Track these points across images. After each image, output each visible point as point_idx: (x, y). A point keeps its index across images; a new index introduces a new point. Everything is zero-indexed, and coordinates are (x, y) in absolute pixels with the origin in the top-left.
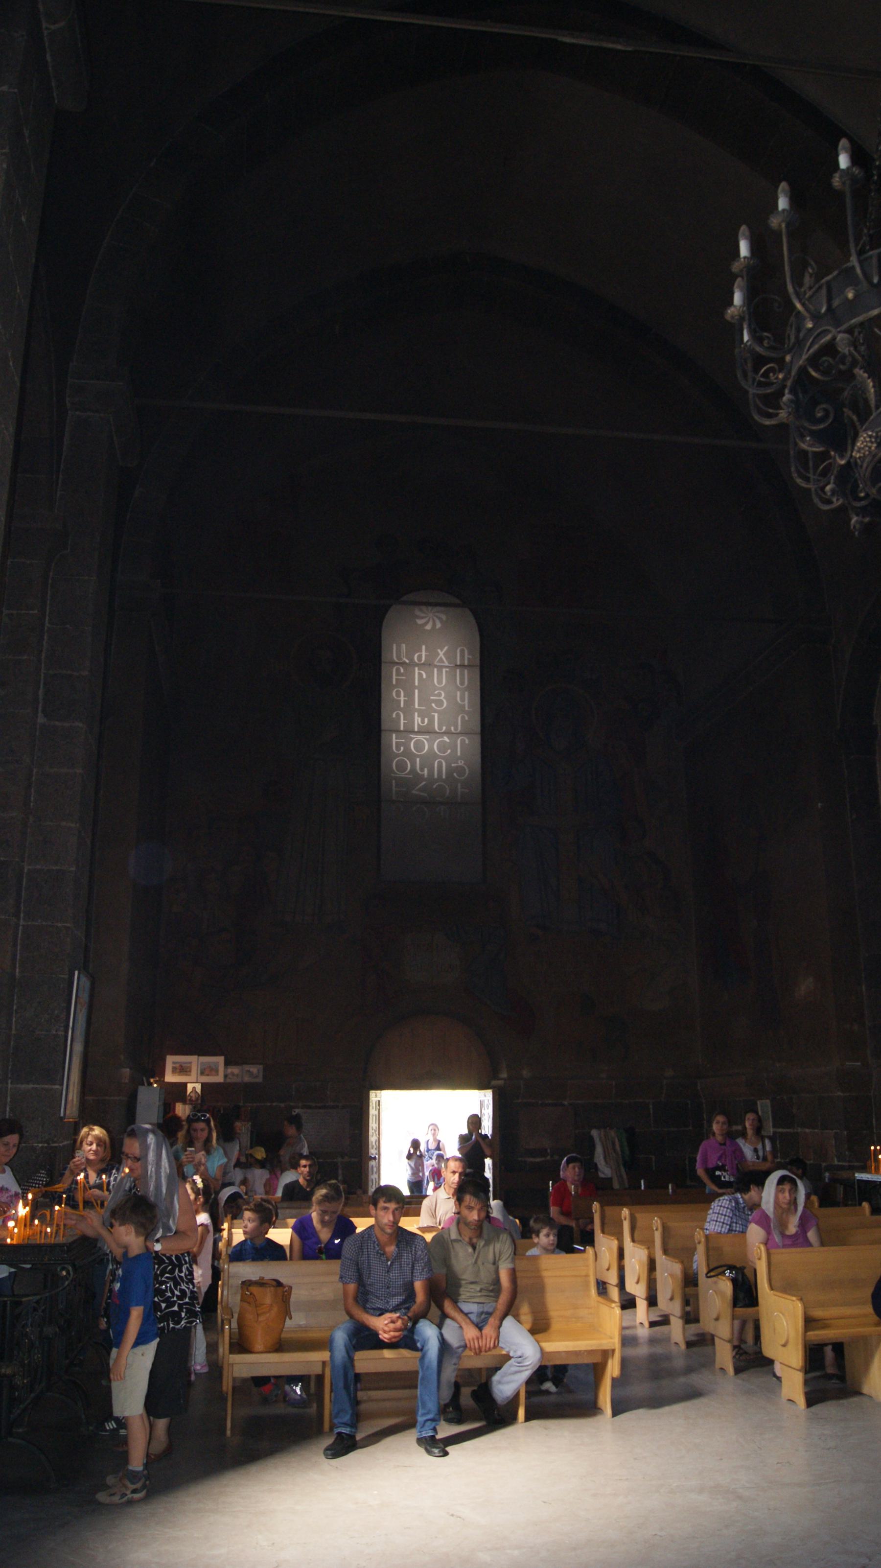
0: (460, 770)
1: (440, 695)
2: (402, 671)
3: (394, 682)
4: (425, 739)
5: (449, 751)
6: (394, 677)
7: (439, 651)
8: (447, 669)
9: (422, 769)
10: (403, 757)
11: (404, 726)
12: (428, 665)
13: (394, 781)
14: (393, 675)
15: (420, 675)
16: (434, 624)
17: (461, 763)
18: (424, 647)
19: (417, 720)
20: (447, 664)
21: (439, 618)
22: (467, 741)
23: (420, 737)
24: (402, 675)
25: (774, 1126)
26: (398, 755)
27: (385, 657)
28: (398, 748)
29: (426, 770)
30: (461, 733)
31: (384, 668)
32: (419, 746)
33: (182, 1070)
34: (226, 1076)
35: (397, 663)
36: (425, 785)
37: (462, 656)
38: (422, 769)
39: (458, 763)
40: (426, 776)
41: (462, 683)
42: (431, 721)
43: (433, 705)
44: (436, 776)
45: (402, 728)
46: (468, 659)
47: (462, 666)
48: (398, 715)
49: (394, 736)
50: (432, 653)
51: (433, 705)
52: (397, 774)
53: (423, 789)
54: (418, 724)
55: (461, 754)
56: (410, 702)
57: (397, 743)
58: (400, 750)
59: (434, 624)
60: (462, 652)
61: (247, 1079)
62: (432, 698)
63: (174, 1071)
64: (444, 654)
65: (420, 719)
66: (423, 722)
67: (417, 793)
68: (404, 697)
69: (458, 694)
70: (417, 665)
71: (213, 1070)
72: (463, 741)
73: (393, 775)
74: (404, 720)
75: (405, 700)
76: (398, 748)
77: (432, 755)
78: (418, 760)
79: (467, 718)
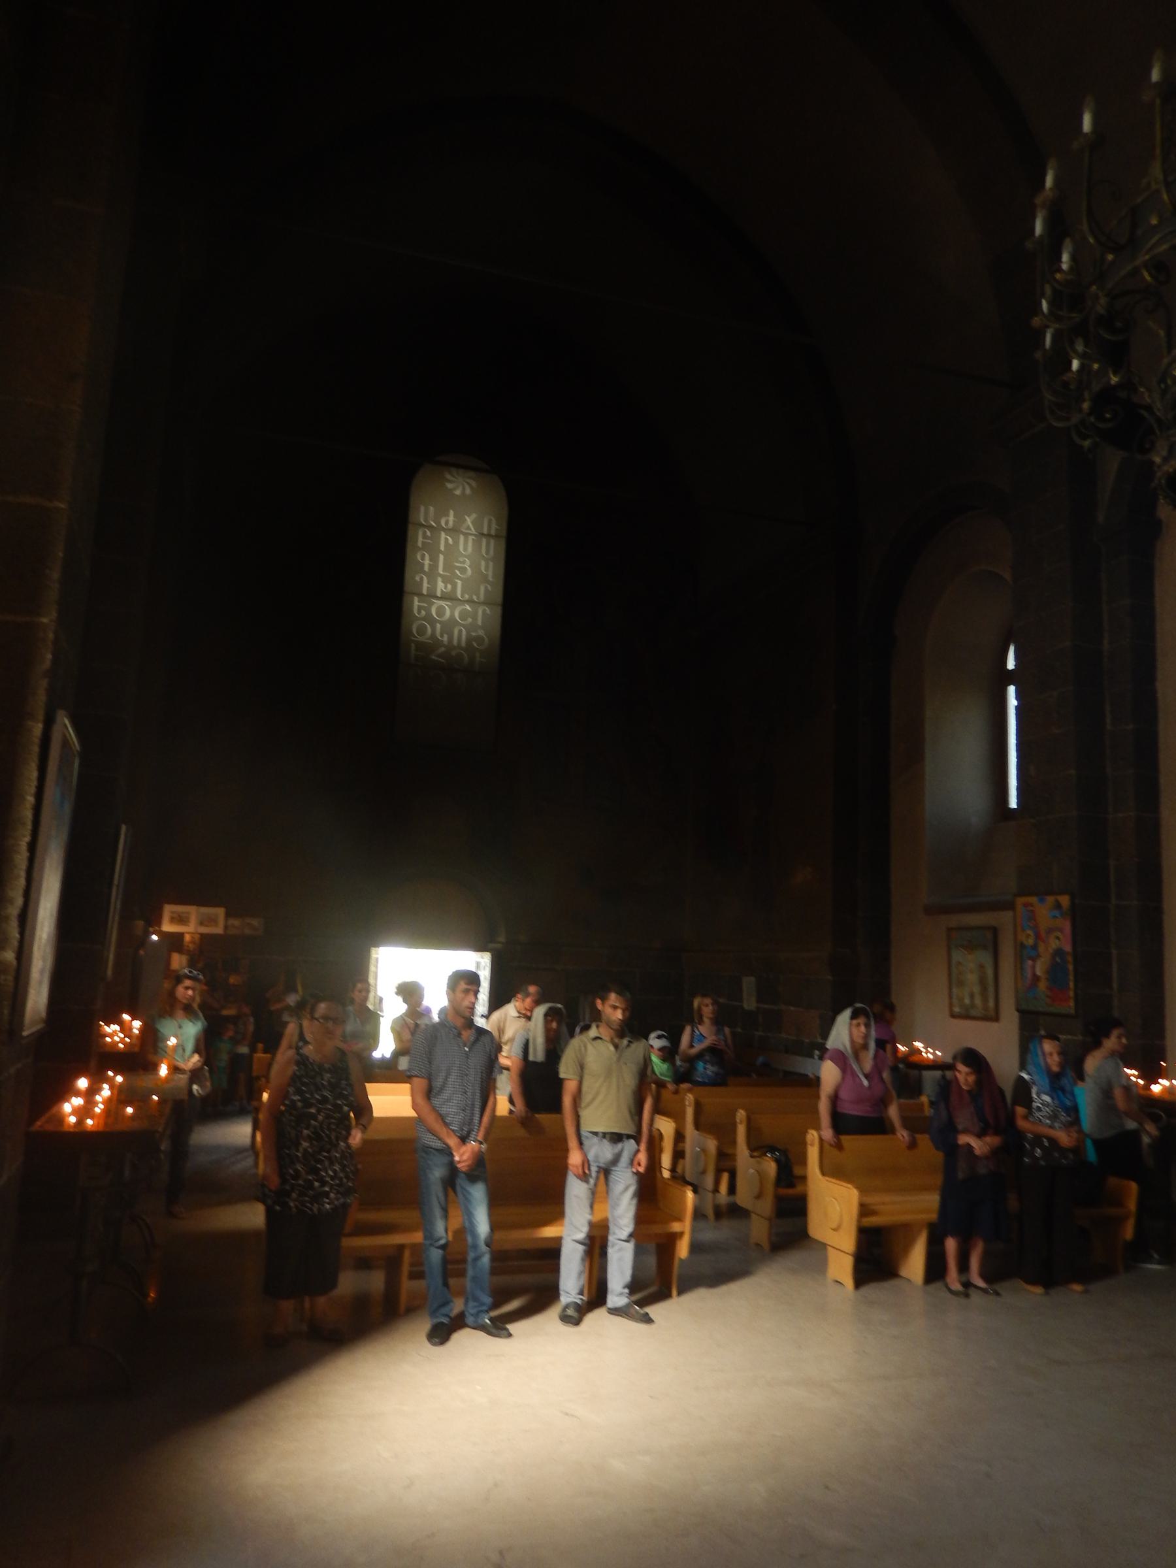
0: (479, 639)
1: (464, 562)
2: (428, 533)
3: (420, 544)
4: (447, 605)
6: (420, 539)
8: (474, 537)
10: (424, 621)
11: (428, 591)
12: (454, 531)
13: (413, 645)
14: (419, 537)
15: (446, 539)
16: (464, 489)
17: (481, 633)
18: (452, 513)
19: (440, 585)
20: (473, 531)
21: (468, 483)
22: (488, 611)
23: (442, 603)
25: (758, 1002)
26: (418, 619)
27: (412, 517)
28: (419, 612)
30: (484, 603)
31: (411, 528)
32: (440, 612)
33: (181, 919)
34: (226, 927)
35: (423, 525)
38: (442, 636)
41: (487, 552)
43: (458, 572)
45: (425, 592)
46: (497, 529)
47: (489, 535)
48: (422, 579)
49: (416, 599)
50: (460, 519)
51: (458, 572)
52: (417, 637)
53: (439, 656)
55: (482, 622)
56: (434, 566)
57: (419, 606)
59: (464, 489)
60: (490, 521)
61: (247, 931)
63: (173, 920)
66: (445, 588)
67: (436, 658)
69: (483, 563)
70: (444, 530)
71: (212, 921)
72: (484, 611)
73: (413, 638)
74: (428, 583)
75: (430, 565)
76: (419, 612)
77: (452, 622)
78: (438, 626)
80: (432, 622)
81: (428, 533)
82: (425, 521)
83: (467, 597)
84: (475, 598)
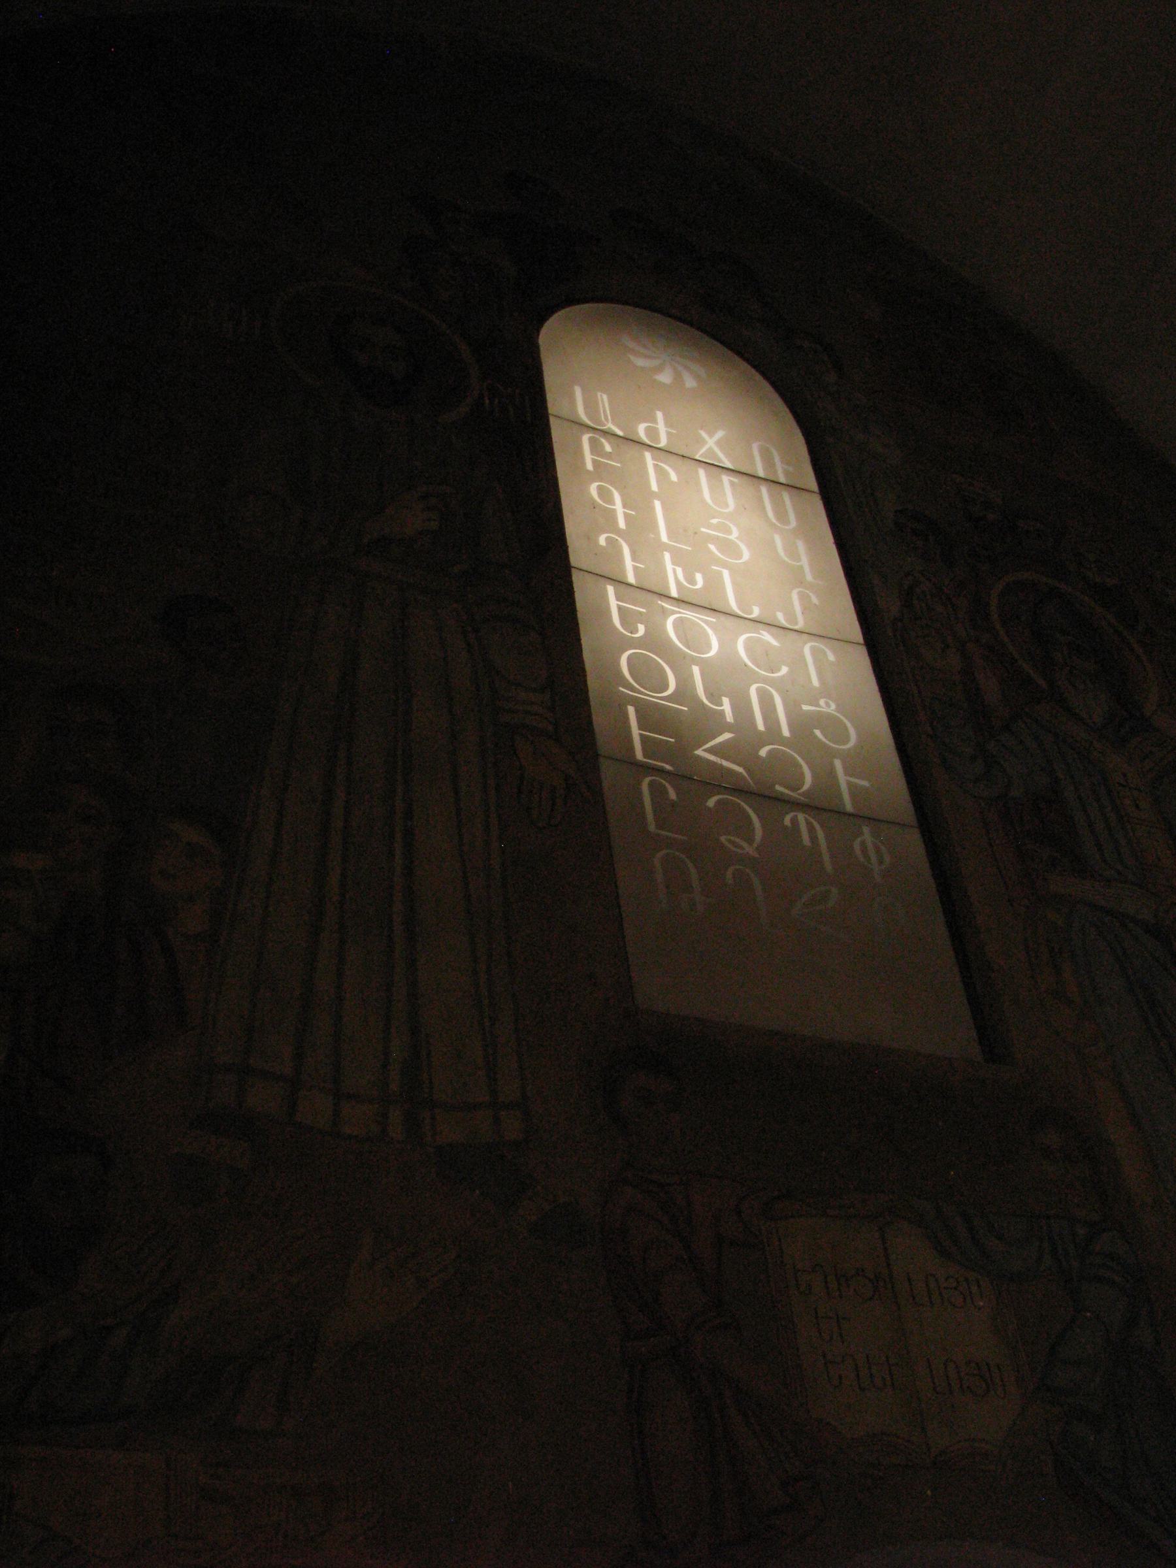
2: (608, 448)
4: (706, 622)
5: (784, 670)
7: (704, 434)
8: (735, 480)
9: (714, 697)
13: (631, 710)
17: (828, 707)
22: (831, 657)
24: (609, 456)
26: (633, 644)
29: (726, 701)
36: (727, 741)
37: (768, 462)
38: (714, 697)
39: (818, 705)
40: (729, 717)
41: (781, 515)
42: (714, 582)
43: (712, 547)
44: (761, 726)
51: (712, 547)
52: (632, 689)
54: (678, 583)
56: (641, 526)
57: (620, 608)
58: (637, 631)
62: (703, 530)
64: (718, 443)
65: (679, 571)
67: (712, 758)
68: (624, 506)
69: (778, 539)
73: (621, 689)
74: (634, 559)
79: (815, 600)
80: (679, 662)
81: (608, 448)
82: (586, 413)
83: (756, 612)
84: (781, 618)
